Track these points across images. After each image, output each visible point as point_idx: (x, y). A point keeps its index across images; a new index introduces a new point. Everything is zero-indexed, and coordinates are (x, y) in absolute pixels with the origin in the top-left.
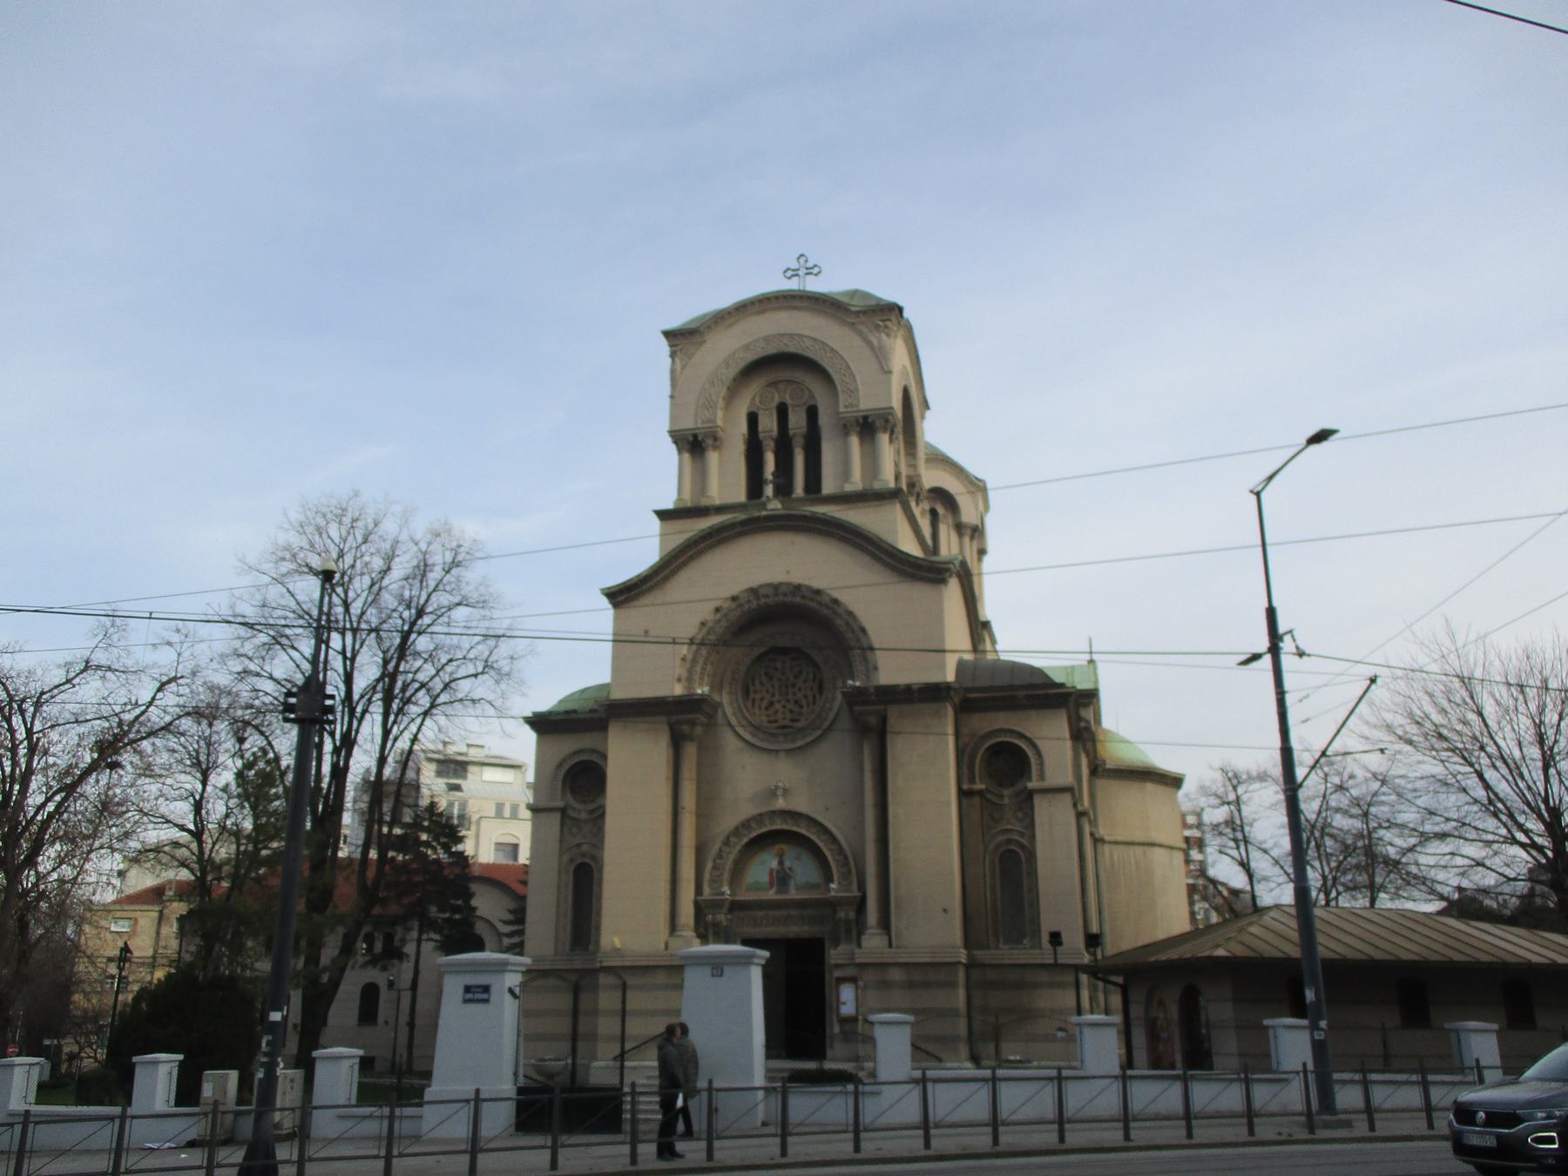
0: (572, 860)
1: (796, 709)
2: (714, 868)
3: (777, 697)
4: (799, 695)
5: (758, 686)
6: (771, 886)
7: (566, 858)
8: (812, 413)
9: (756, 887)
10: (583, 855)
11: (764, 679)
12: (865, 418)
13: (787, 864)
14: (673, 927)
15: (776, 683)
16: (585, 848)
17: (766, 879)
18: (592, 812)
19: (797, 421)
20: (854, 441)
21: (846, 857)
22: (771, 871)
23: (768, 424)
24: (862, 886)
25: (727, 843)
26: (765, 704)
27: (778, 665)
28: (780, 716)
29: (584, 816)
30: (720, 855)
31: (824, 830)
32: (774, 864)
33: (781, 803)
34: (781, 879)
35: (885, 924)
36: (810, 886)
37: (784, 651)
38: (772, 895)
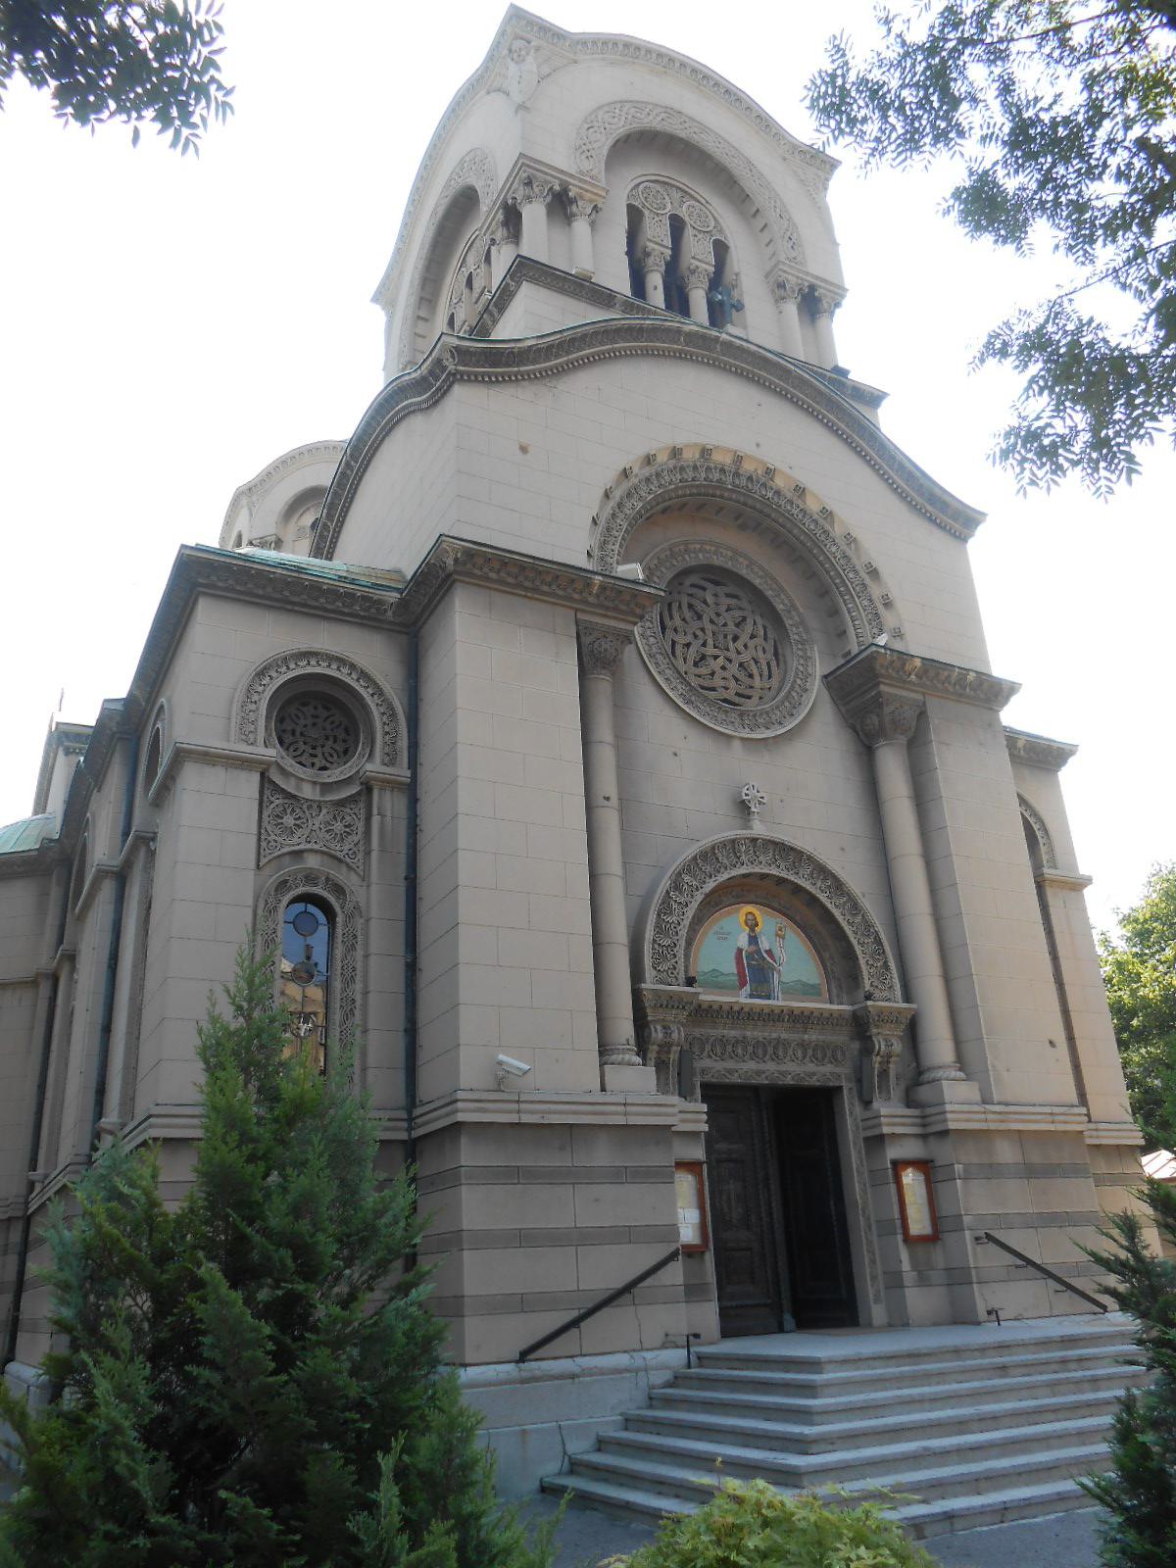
0: (282, 886)
4: (746, 657)
6: (743, 984)
9: (716, 983)
10: (310, 878)
11: (688, 615)
13: (764, 944)
15: (709, 627)
16: (312, 862)
17: (731, 967)
18: (326, 787)
21: (878, 941)
22: (740, 951)
27: (710, 600)
29: (308, 792)
32: (743, 941)
33: (758, 829)
34: (756, 969)
36: (808, 990)
37: (717, 575)
38: (743, 998)
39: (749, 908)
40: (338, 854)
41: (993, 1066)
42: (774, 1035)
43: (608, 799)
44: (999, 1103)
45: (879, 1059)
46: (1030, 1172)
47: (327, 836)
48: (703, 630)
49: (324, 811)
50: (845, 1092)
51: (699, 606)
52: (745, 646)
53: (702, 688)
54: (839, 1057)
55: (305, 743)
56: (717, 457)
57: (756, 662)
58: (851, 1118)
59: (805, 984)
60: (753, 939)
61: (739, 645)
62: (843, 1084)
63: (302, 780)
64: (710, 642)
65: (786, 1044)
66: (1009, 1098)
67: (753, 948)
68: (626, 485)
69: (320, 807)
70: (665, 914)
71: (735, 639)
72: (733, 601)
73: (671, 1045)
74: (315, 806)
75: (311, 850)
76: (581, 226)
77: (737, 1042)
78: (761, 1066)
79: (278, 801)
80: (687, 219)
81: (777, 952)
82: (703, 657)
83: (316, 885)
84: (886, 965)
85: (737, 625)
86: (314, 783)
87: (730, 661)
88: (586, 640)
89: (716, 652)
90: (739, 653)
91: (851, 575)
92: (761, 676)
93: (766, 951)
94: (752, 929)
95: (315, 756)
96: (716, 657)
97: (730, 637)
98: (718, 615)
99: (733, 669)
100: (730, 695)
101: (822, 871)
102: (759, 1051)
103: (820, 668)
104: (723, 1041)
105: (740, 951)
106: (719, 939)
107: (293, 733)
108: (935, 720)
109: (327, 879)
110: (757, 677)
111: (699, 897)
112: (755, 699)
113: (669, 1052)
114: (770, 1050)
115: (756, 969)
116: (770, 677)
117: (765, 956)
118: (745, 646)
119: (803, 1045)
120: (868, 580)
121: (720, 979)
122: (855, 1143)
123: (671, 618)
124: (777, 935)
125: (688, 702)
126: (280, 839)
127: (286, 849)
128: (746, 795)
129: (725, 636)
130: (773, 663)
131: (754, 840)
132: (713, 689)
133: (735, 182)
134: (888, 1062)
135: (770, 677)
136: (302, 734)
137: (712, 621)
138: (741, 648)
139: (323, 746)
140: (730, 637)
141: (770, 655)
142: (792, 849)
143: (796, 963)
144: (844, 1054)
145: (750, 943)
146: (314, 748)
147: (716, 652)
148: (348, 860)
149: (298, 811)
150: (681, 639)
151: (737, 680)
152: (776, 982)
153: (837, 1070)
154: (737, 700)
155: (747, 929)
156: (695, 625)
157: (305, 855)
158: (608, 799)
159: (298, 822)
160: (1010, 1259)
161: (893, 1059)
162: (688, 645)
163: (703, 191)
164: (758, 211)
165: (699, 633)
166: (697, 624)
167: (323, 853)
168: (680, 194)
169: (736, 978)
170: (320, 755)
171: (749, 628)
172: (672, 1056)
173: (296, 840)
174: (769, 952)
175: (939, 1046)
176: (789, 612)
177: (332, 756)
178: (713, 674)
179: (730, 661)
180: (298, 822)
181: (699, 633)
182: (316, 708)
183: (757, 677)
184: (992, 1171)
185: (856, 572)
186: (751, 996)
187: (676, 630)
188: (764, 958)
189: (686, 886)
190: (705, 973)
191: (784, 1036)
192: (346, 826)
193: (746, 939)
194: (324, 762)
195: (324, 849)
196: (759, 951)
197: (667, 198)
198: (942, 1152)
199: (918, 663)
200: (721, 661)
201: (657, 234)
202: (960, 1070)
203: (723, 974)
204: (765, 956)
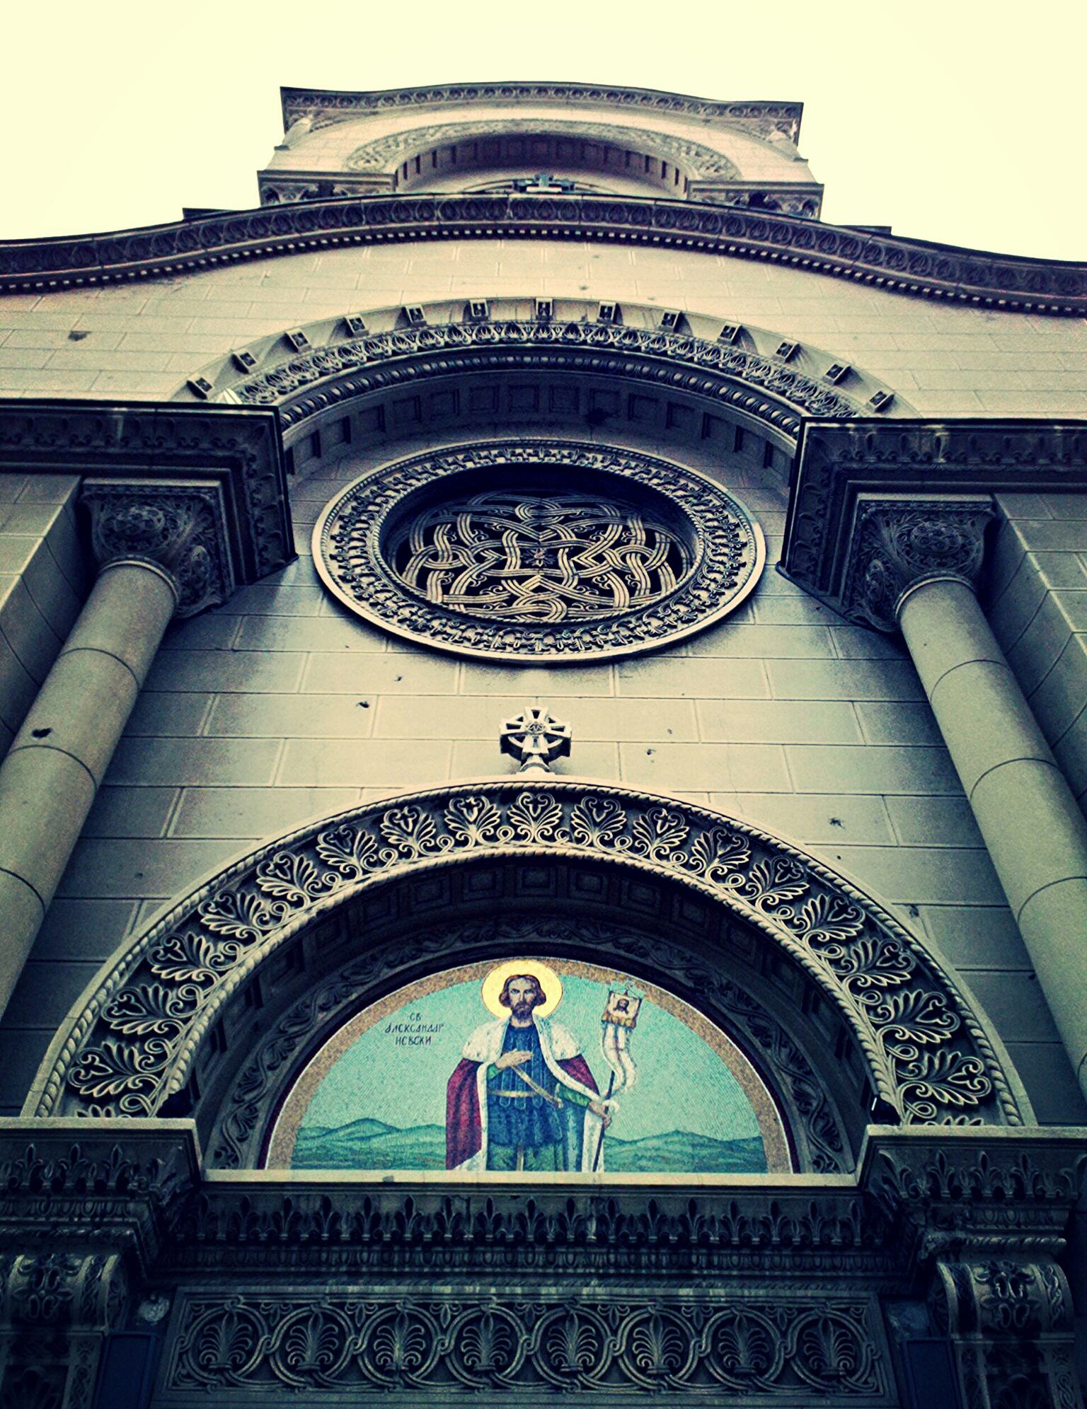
2: (129, 1003)
21: (925, 974)
22: (468, 1068)
32: (485, 1044)
42: (551, 1292)
54: (834, 1361)
59: (698, 1142)
60: (522, 1035)
65: (595, 1322)
70: (167, 964)
73: (65, 1317)
77: (393, 1319)
82: (495, 581)
84: (964, 1038)
93: (563, 1063)
94: (522, 1012)
96: (521, 579)
104: (332, 1329)
105: (468, 1068)
106: (401, 1041)
113: (61, 1348)
114: (528, 1342)
117: (558, 1072)
119: (669, 1321)
121: (376, 1143)
124: (606, 1022)
133: (628, 153)
144: (849, 1345)
145: (507, 1047)
161: (1046, 1339)
162: (458, 571)
164: (664, 164)
169: (443, 1138)
172: (73, 1360)
174: (575, 1065)
181: (492, 556)
190: (330, 1131)
191: (594, 1290)
193: (499, 1035)
196: (537, 1066)
203: (391, 1129)
204: (558, 1072)
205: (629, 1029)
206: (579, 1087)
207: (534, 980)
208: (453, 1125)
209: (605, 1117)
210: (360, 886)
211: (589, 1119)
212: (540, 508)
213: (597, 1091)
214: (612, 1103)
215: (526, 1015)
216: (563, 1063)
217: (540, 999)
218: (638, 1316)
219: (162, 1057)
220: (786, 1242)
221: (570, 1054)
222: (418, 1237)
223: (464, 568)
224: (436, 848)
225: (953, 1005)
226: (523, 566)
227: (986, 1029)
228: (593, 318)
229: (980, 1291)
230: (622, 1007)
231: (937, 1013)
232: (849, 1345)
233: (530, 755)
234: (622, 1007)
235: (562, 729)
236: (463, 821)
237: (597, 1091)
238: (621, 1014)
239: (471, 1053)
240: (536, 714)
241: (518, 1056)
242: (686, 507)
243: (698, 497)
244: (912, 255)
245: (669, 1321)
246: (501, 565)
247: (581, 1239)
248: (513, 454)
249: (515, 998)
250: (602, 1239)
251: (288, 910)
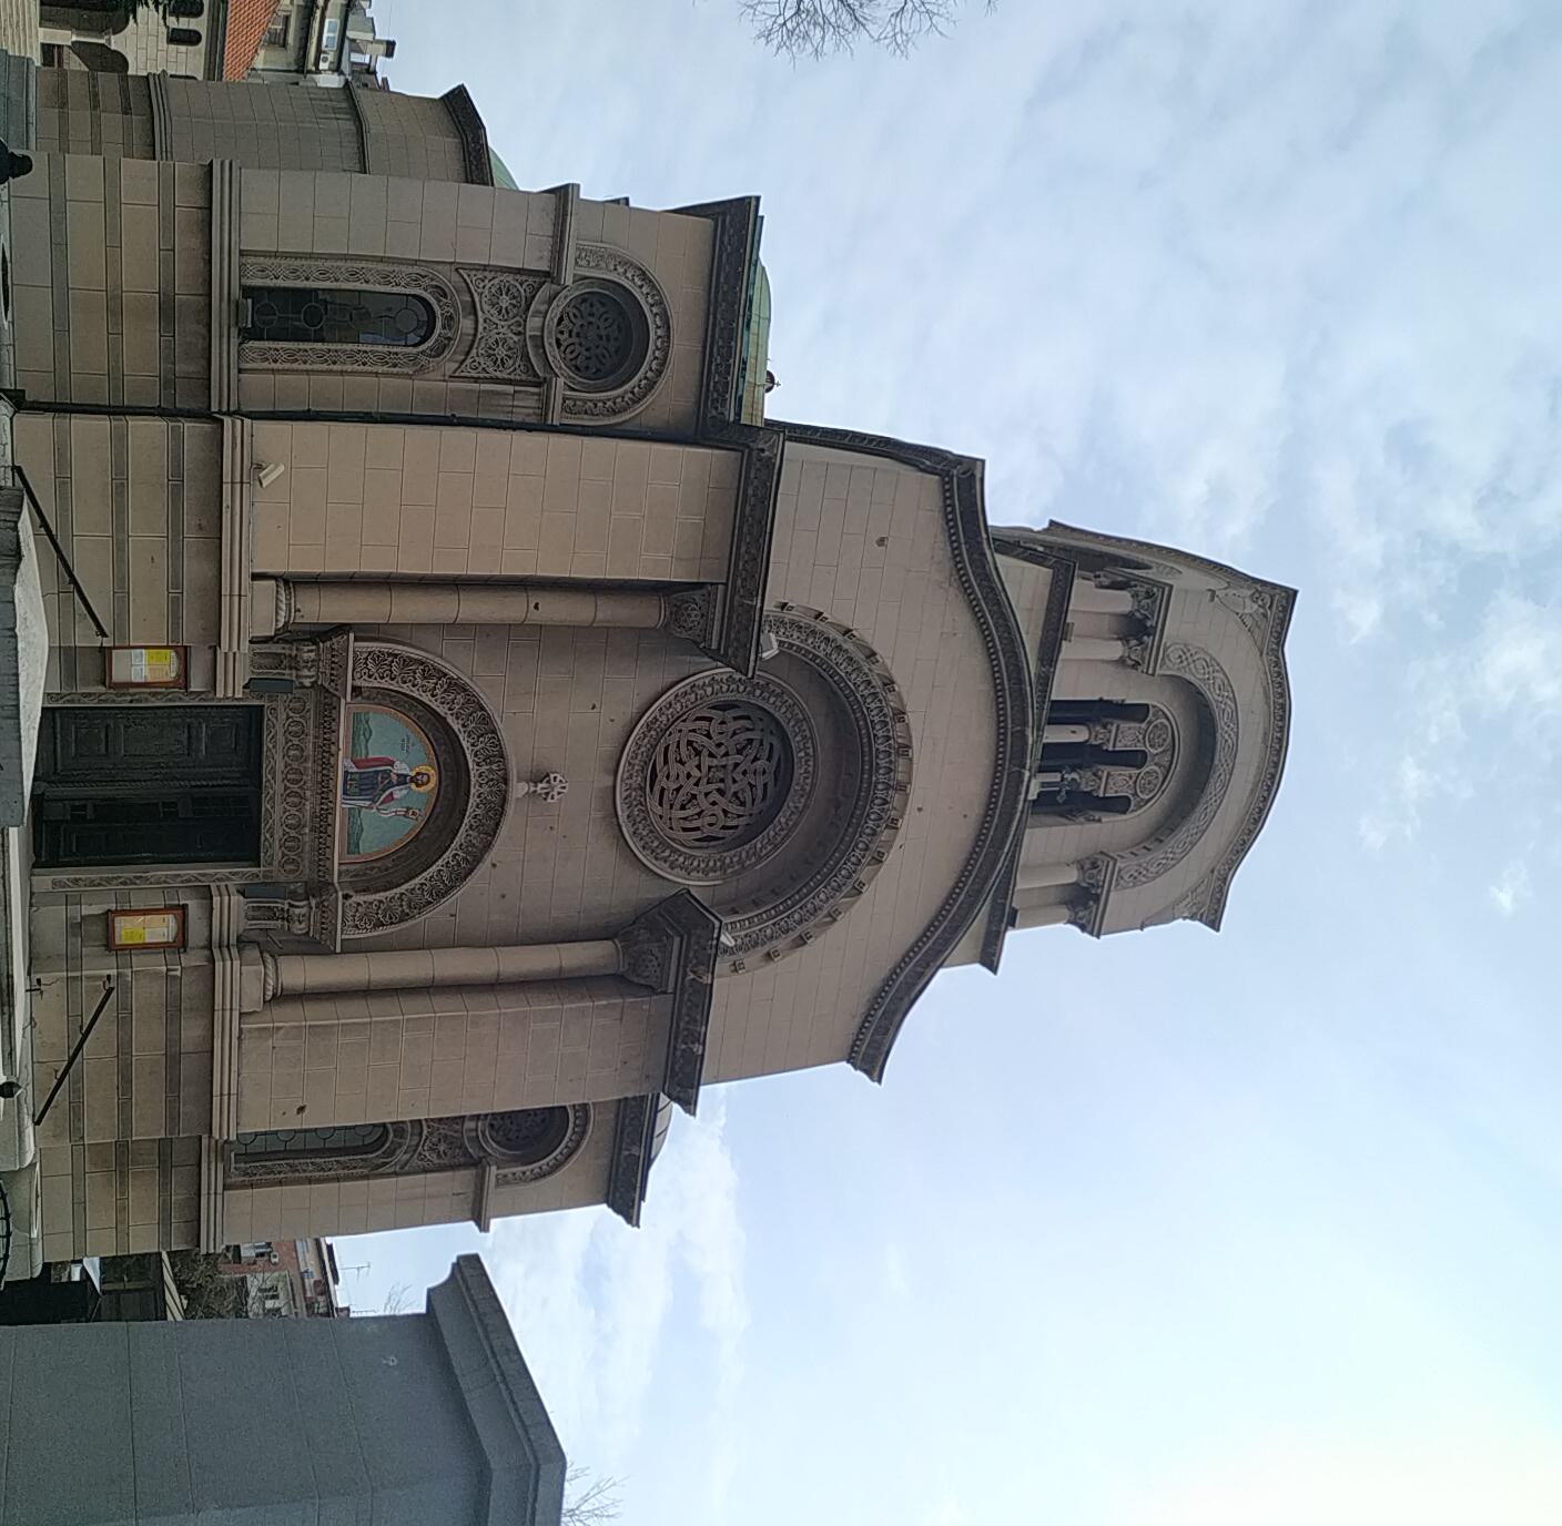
0: (442, 293)
1: (681, 797)
2: (407, 662)
3: (706, 761)
4: (704, 803)
5: (733, 725)
7: (449, 279)
8: (1119, 805)
9: (359, 731)
10: (450, 321)
11: (743, 737)
12: (1097, 898)
13: (399, 793)
14: (291, 582)
15: (731, 761)
16: (466, 324)
18: (539, 342)
19: (1117, 781)
20: (1072, 876)
21: (404, 917)
23: (1126, 736)
24: (352, 948)
25: (455, 686)
26: (700, 739)
28: (674, 768)
29: (533, 323)
30: (430, 672)
31: (461, 875)
32: (401, 768)
33: (519, 789)
34: (373, 782)
35: (282, 997)
37: (784, 773)
38: (343, 763)
39: (434, 780)
40: (474, 351)
41: (279, 1028)
42: (308, 793)
43: (536, 607)
44: (241, 1030)
45: (286, 907)
46: (173, 1059)
47: (491, 341)
48: (726, 754)
49: (516, 338)
50: (255, 870)
51: (751, 752)
52: (714, 803)
53: (667, 749)
54: (288, 867)
55: (582, 325)
56: (901, 763)
57: (699, 814)
58: (226, 877)
61: (715, 796)
62: (262, 869)
63: (545, 318)
64: (715, 762)
65: (299, 807)
66: (245, 1044)
67: (394, 778)
68: (859, 656)
69: (519, 333)
70: (424, 671)
71: (721, 792)
72: (760, 792)
74: (521, 329)
75: (476, 322)
76: (1116, 650)
77: (302, 750)
78: (279, 777)
79: (522, 291)
80: (1145, 769)
81: (393, 807)
82: (698, 753)
83: (444, 328)
85: (735, 794)
86: (543, 331)
87: (697, 784)
88: (697, 595)
89: (705, 769)
90: (707, 794)
91: (797, 916)
92: (685, 819)
93: (391, 794)
95: (570, 336)
96: (699, 767)
97: (722, 785)
98: (745, 773)
99: (689, 787)
100: (661, 781)
101: (474, 858)
102: (294, 776)
103: (696, 884)
105: (392, 763)
107: (592, 315)
108: (647, 1004)
109: (449, 339)
110: (683, 814)
111: (442, 710)
112: (658, 810)
114: (295, 787)
115: (373, 782)
116: (685, 830)
117: (387, 792)
118: (714, 803)
119: (299, 826)
120: (793, 935)
122: (204, 875)
123: (735, 719)
124: (408, 809)
125: (649, 727)
126: (486, 292)
127: (477, 299)
128: (555, 778)
129: (722, 781)
130: (698, 835)
131: (506, 781)
132: (666, 762)
134: (283, 919)
135: (685, 830)
136: (590, 323)
137: (736, 765)
138: (711, 798)
139: (580, 344)
140: (722, 785)
141: (707, 831)
142: (497, 825)
143: (384, 825)
146: (578, 335)
147: (705, 769)
148: (469, 361)
149: (515, 311)
150: (714, 728)
151: (678, 790)
152: (361, 803)
153: (275, 863)
154: (657, 788)
155: (413, 774)
156: (731, 745)
157: (472, 317)
158: (536, 607)
159: (504, 311)
160: (87, 1022)
161: (286, 923)
162: (708, 736)
163: (1172, 785)
165: (723, 750)
166: (732, 751)
167: (475, 335)
168: (1167, 764)
170: (570, 341)
171: (734, 808)
173: (486, 307)
175: (299, 972)
176: (754, 854)
177: (572, 353)
178: (683, 763)
179: (697, 784)
180: (504, 311)
181: (723, 750)
182: (616, 339)
183: (683, 814)
184: (173, 1012)
185: (800, 922)
186: (346, 773)
187: (723, 723)
188: (384, 791)
189: (452, 696)
190: (367, 722)
192: (502, 360)
194: (566, 344)
195: (479, 336)
197: (1160, 750)
198: (194, 958)
199: (707, 980)
200: (695, 773)
201: (1126, 736)
202: (274, 995)
203: (367, 741)
205: (404, 816)
206: (382, 798)
207: (428, 781)
208: (367, 760)
209: (370, 807)
210: (456, 730)
211: (368, 803)
212: (764, 772)
213: (382, 803)
214: (375, 810)
215: (412, 781)
216: (391, 794)
217: (418, 785)
218: (301, 815)
219: (382, 678)
220: (320, 860)
221: (395, 796)
222: (324, 757)
223: (710, 738)
224: (476, 755)
225: (392, 923)
226: (710, 767)
227: (380, 931)
228: (893, 813)
229: (297, 911)
230: (413, 813)
231: (391, 918)
232: (291, 872)
233: (536, 786)
234: (413, 813)
235: (552, 798)
236: (491, 763)
237: (382, 803)
238: (411, 812)
239: (397, 763)
240: (564, 788)
241: (394, 778)
242: (747, 847)
243: (754, 854)
244: (915, 985)
245: (299, 826)
246: (711, 755)
247: (322, 803)
248: (807, 761)
249: (419, 777)
250: (322, 809)
251: (447, 707)
